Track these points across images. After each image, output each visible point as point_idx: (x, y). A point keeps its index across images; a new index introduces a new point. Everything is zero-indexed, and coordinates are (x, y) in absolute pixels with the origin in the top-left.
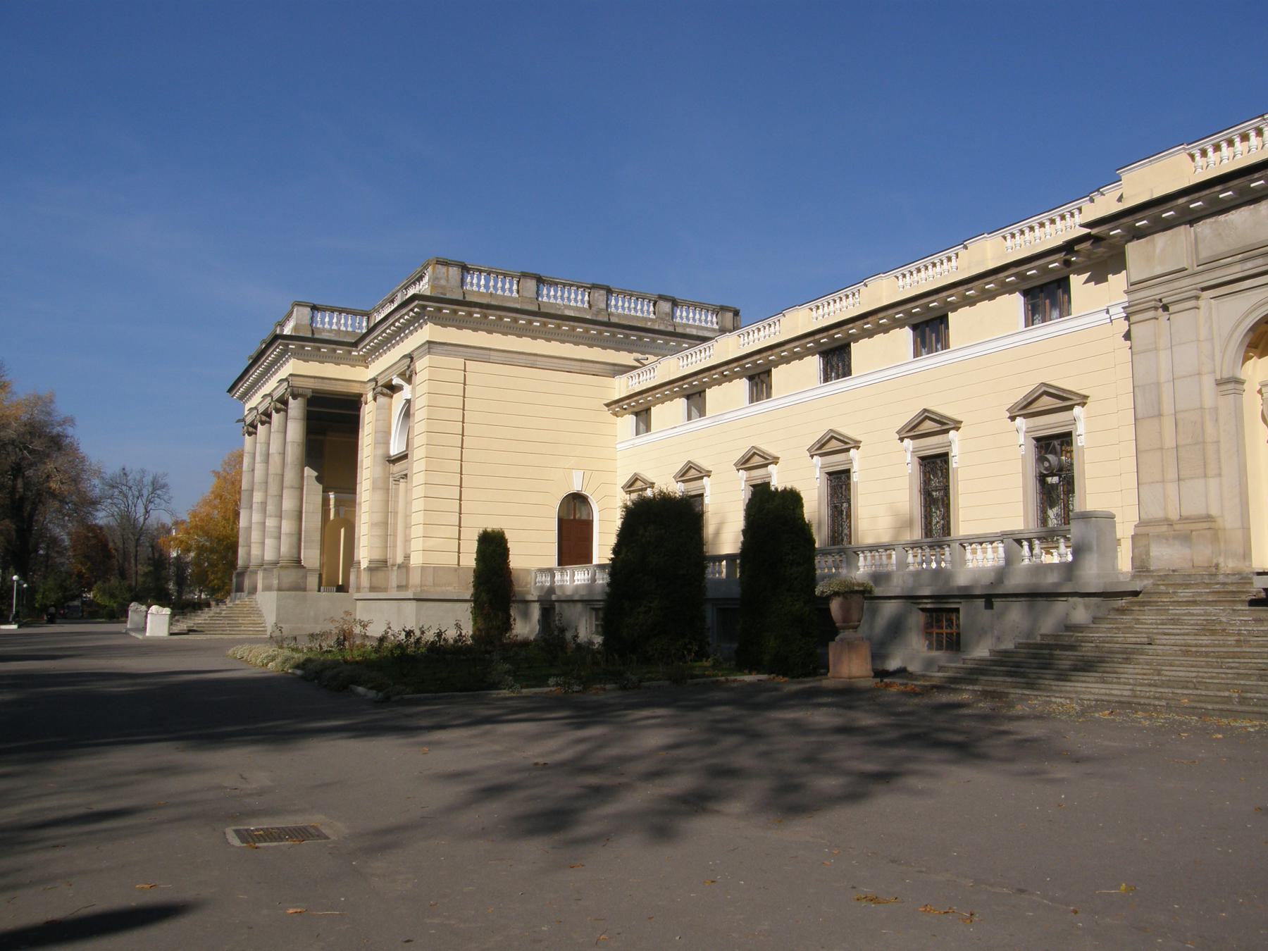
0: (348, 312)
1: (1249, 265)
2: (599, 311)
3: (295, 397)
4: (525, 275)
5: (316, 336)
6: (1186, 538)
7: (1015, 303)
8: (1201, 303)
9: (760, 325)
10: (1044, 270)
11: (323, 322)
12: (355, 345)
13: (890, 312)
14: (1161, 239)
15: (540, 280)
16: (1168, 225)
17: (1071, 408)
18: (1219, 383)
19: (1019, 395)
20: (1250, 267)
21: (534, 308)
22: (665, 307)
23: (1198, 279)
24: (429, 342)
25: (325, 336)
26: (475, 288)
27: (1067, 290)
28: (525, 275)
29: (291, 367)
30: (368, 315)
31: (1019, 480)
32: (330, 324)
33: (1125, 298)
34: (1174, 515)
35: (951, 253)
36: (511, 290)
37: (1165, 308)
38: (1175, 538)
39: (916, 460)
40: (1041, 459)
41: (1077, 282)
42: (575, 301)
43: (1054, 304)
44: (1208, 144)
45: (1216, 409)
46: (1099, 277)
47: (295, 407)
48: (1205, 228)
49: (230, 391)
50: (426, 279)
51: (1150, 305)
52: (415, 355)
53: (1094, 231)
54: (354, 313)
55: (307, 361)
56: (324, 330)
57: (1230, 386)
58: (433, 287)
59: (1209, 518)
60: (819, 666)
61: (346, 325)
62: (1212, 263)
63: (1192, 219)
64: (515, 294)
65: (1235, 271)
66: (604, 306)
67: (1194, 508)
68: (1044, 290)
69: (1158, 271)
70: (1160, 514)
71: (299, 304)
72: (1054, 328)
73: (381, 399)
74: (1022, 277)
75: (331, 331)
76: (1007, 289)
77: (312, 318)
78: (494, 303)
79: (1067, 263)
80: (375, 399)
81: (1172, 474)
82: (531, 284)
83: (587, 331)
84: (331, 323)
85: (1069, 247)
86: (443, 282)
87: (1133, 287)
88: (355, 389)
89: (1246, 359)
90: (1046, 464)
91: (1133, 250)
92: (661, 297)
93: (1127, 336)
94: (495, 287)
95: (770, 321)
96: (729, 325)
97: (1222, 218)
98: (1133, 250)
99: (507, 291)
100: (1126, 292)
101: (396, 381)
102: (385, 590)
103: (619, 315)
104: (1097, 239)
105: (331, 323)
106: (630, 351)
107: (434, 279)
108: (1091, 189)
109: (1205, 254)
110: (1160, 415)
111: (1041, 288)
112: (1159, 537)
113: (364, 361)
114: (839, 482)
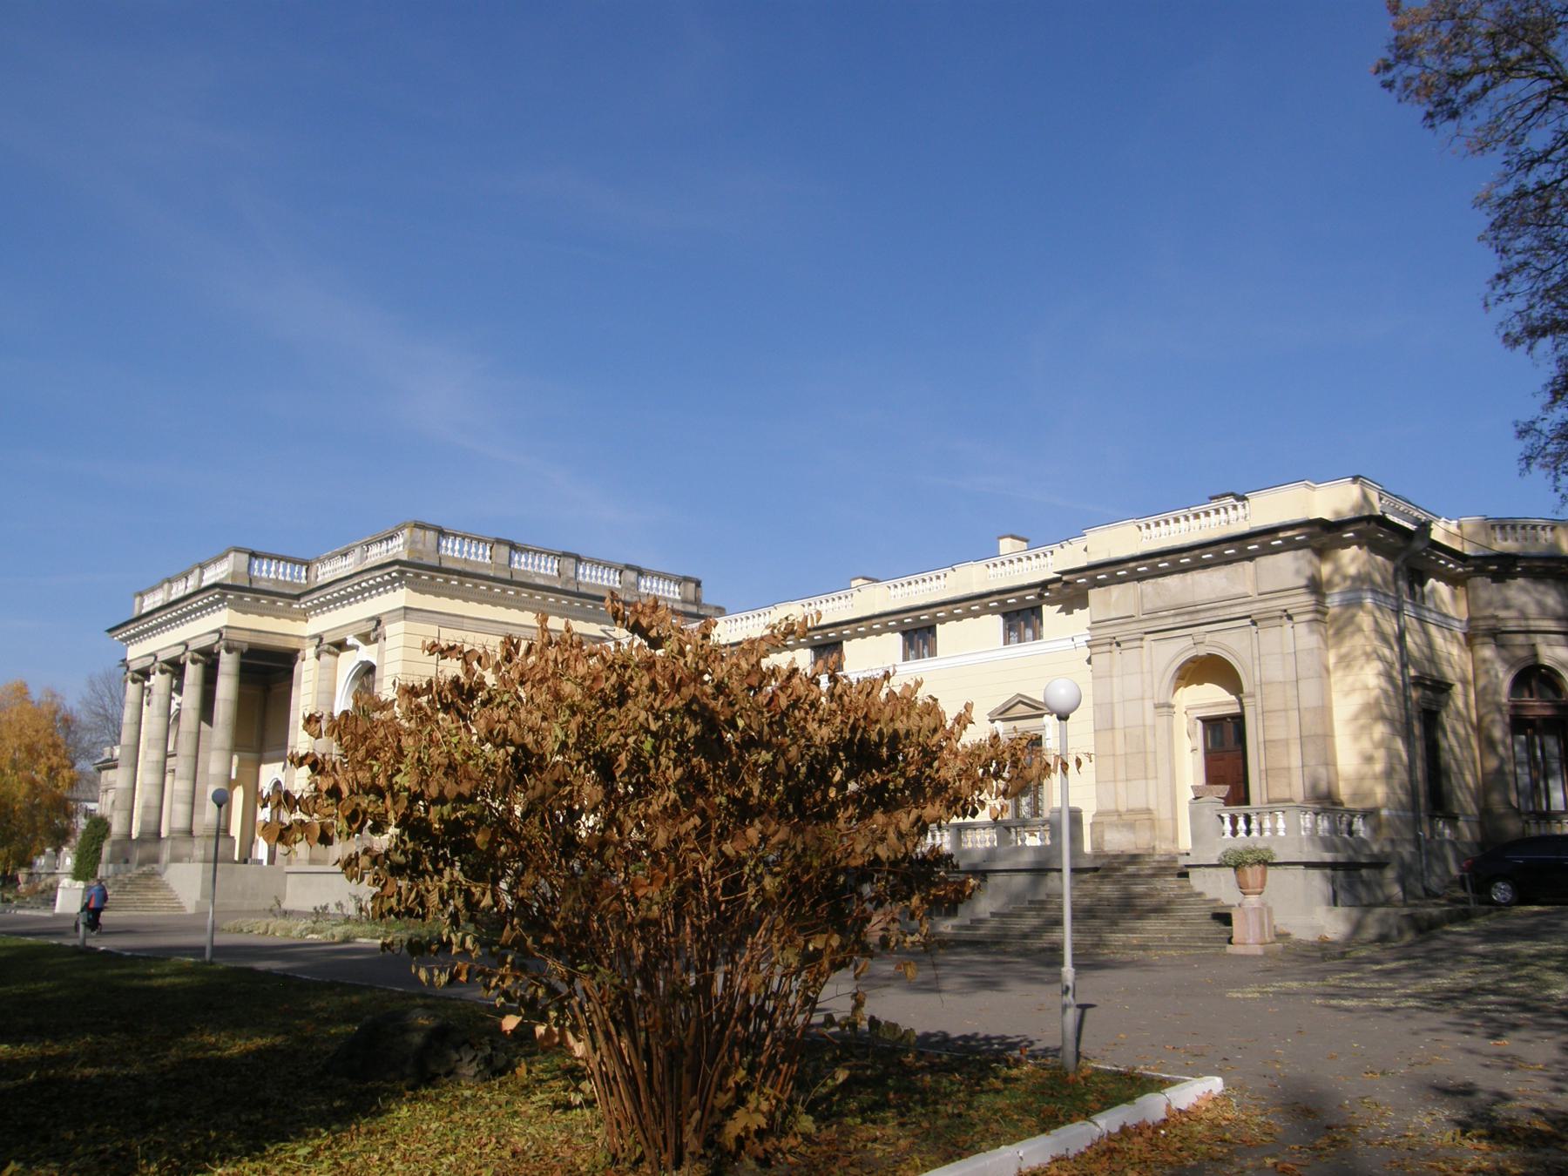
0: (287, 560)
1: (1179, 619)
2: (568, 580)
3: (229, 650)
4: (499, 541)
5: (255, 586)
6: (1131, 826)
7: (995, 623)
8: (1144, 643)
9: (749, 614)
10: (1022, 599)
11: (260, 570)
12: (298, 597)
13: (884, 619)
14: (1116, 590)
15: (513, 547)
16: (1122, 580)
17: (1041, 716)
18: (1157, 707)
19: (999, 702)
20: (1179, 621)
21: (507, 576)
22: (631, 576)
23: (1143, 625)
24: (406, 608)
25: (263, 585)
26: (449, 553)
27: (1040, 616)
28: (499, 541)
29: (223, 617)
30: (308, 564)
32: (267, 572)
34: (1122, 808)
35: (940, 573)
36: (484, 556)
37: (1118, 644)
38: (1124, 826)
41: (1049, 612)
42: (544, 568)
43: (1026, 626)
44: (1151, 521)
45: (1154, 726)
46: (1068, 609)
47: (228, 663)
48: (1148, 586)
49: (110, 631)
50: (400, 540)
51: (1105, 641)
52: (383, 618)
53: (1065, 578)
54: (294, 562)
55: (245, 613)
56: (261, 579)
58: (411, 551)
59: (1148, 811)
61: (284, 574)
62: (1153, 614)
63: (1141, 578)
64: (487, 560)
65: (1169, 623)
66: (572, 574)
67: (1139, 804)
68: (1020, 613)
70: (1112, 807)
71: (237, 550)
72: (1029, 648)
73: (325, 658)
74: (1003, 603)
75: (269, 580)
76: (987, 610)
77: (250, 565)
78: (468, 569)
79: (1041, 596)
80: (318, 657)
81: (1121, 776)
82: (505, 550)
83: (570, 603)
84: (268, 572)
85: (1044, 585)
86: (420, 546)
87: (1096, 624)
88: (293, 644)
89: (1176, 689)
91: (1094, 594)
92: (628, 567)
93: (1089, 661)
94: (469, 552)
95: (760, 611)
96: (691, 597)
97: (1160, 580)
98: (1094, 594)
99: (480, 556)
101: (351, 641)
102: (324, 862)
103: (587, 584)
104: (1067, 583)
105: (268, 572)
106: (599, 623)
107: (411, 544)
108: (1063, 538)
109: (1148, 606)
110: (1113, 728)
111: (1018, 612)
112: (1112, 825)
113: (305, 615)
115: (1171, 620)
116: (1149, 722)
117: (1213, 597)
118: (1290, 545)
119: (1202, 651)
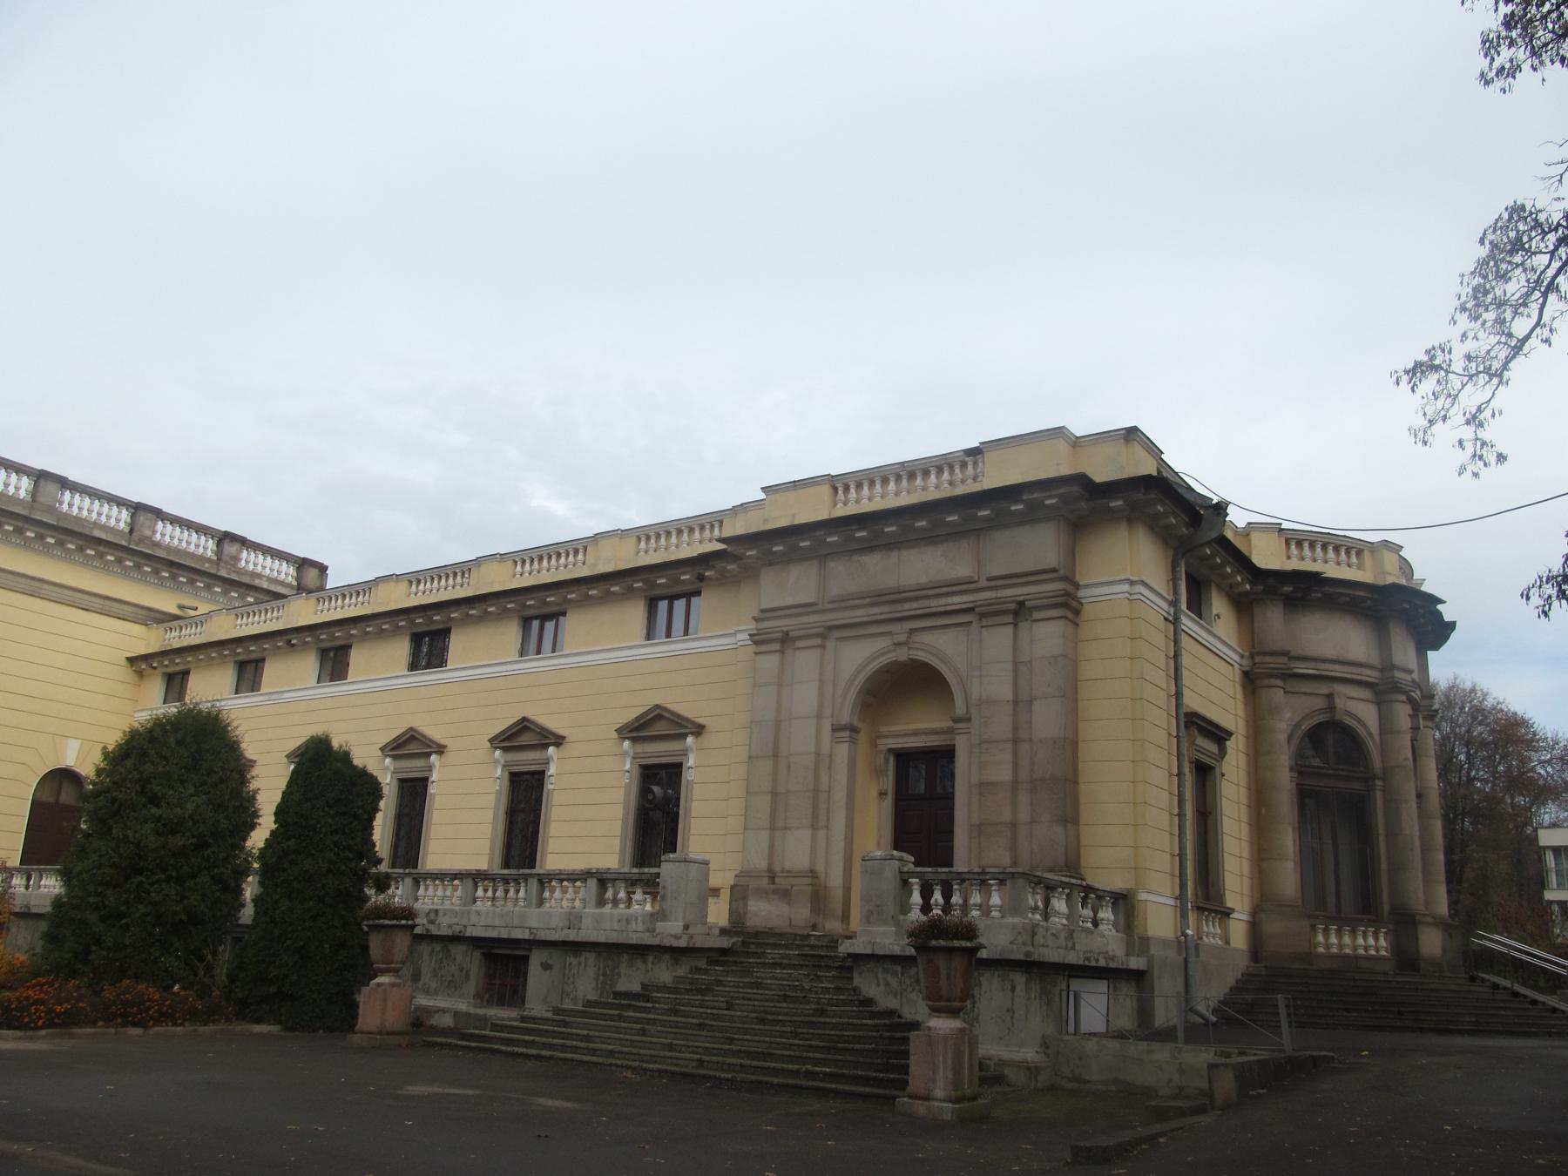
1: (876, 610)
6: (785, 894)
18: (835, 729)
31: (619, 812)
33: (753, 625)
38: (775, 892)
39: (506, 775)
40: (644, 791)
51: (774, 639)
57: (847, 734)
60: (344, 1017)
62: (843, 602)
65: (860, 615)
69: (789, 601)
85: (704, 560)
90: (650, 797)
100: (756, 620)
114: (414, 792)
115: (861, 612)
116: (825, 749)
117: (923, 580)
118: (1035, 514)
119: (902, 655)
